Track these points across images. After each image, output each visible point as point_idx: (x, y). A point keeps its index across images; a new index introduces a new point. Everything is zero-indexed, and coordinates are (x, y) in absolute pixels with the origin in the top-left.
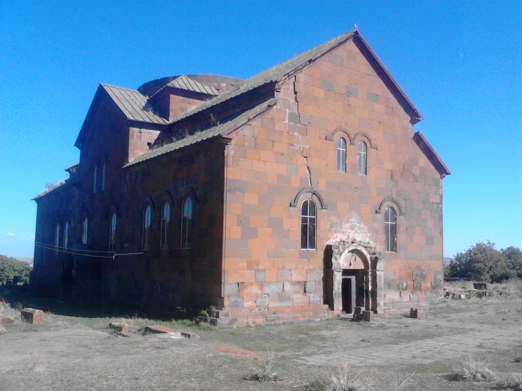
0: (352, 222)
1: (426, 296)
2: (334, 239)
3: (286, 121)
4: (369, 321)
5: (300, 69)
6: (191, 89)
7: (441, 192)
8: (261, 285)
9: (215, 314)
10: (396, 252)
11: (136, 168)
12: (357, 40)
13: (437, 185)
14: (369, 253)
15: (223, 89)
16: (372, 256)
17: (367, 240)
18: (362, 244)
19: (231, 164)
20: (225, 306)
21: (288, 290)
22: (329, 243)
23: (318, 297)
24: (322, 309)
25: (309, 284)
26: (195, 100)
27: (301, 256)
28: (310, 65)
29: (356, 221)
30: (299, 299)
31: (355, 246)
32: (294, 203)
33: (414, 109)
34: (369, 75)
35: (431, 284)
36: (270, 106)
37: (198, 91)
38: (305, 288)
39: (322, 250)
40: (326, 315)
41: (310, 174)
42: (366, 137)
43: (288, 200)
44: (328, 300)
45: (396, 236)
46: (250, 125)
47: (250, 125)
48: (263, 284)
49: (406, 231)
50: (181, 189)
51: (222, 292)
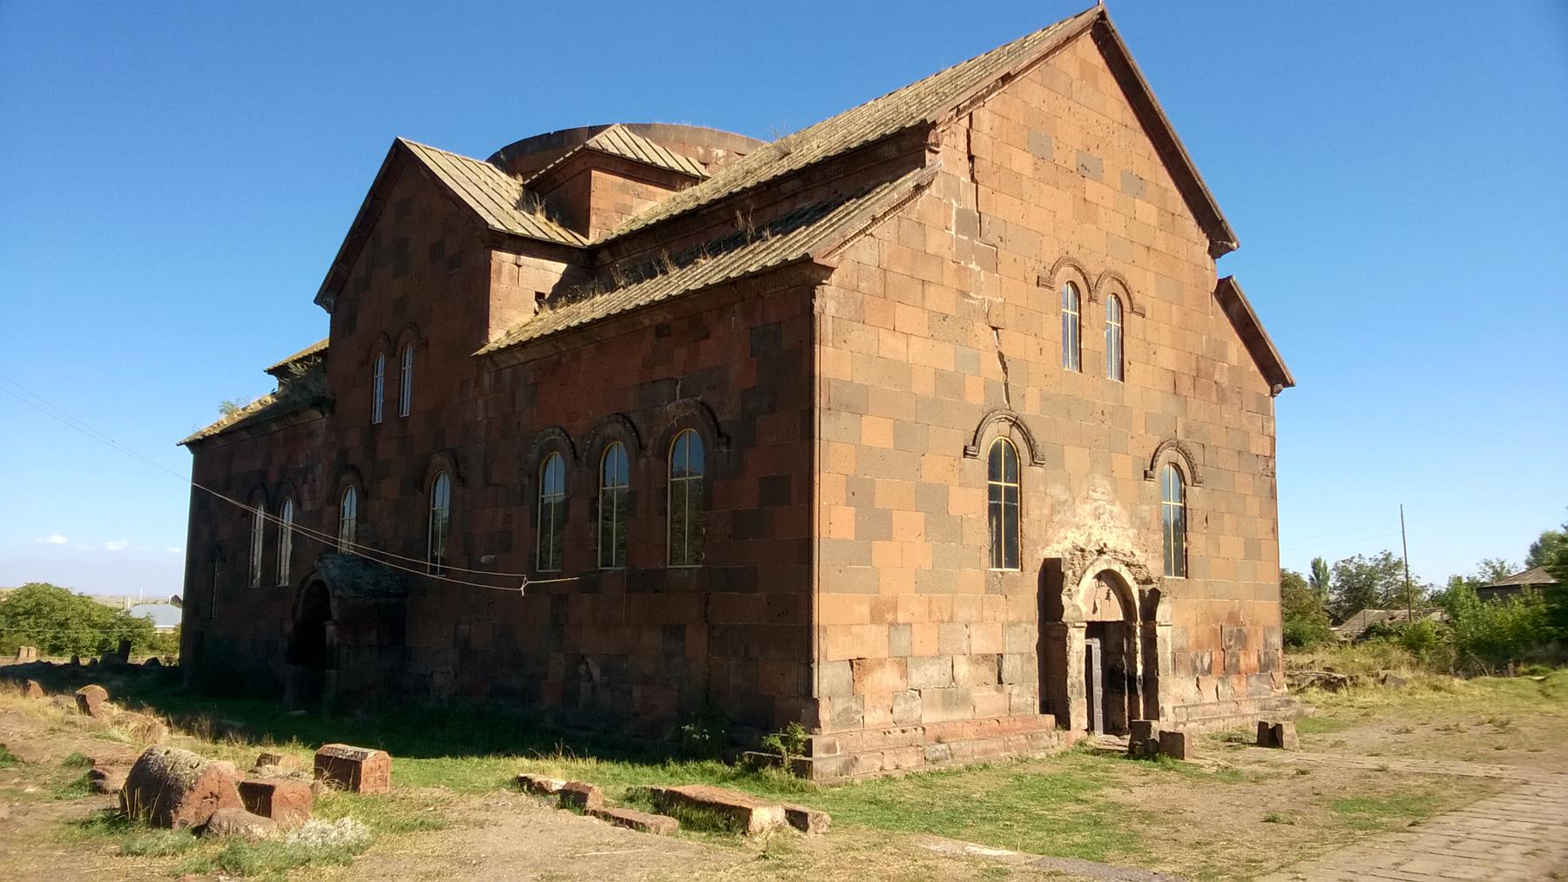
0: (1096, 500)
1: (1249, 688)
2: (1058, 542)
3: (951, 230)
4: (1183, 759)
5: (983, 97)
6: (646, 159)
7: (1272, 429)
8: (903, 665)
9: (800, 747)
10: (1187, 577)
11: (518, 355)
12: (1102, 33)
13: (1265, 411)
14: (1135, 579)
15: (716, 164)
16: (1142, 587)
17: (1128, 547)
18: (1121, 556)
19: (830, 337)
20: (822, 725)
21: (964, 677)
22: (1051, 552)
23: (1027, 694)
24: (1041, 727)
25: (1010, 661)
26: (651, 188)
27: (990, 588)
28: (1004, 89)
29: (1104, 498)
30: (987, 700)
31: (1107, 562)
32: (974, 448)
33: (1220, 219)
34: (1126, 126)
35: (1259, 660)
36: (919, 188)
37: (661, 163)
38: (999, 674)
39: (1035, 571)
40: (1055, 740)
41: (1006, 373)
42: (1121, 283)
43: (961, 439)
44: (1053, 702)
45: (1186, 537)
46: (872, 235)
47: (871, 235)
48: (909, 662)
49: (1205, 525)
50: (670, 408)
51: (815, 685)
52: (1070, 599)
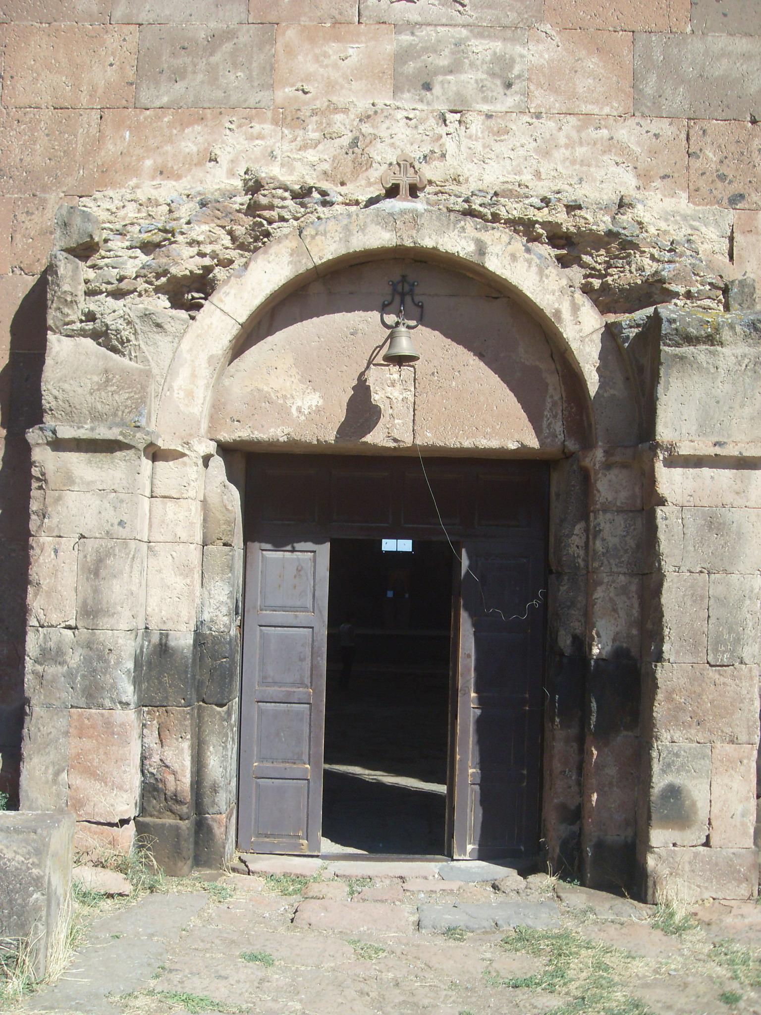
0: (412, 27)
2: (162, 172)
18: (512, 209)
52: (114, 350)
